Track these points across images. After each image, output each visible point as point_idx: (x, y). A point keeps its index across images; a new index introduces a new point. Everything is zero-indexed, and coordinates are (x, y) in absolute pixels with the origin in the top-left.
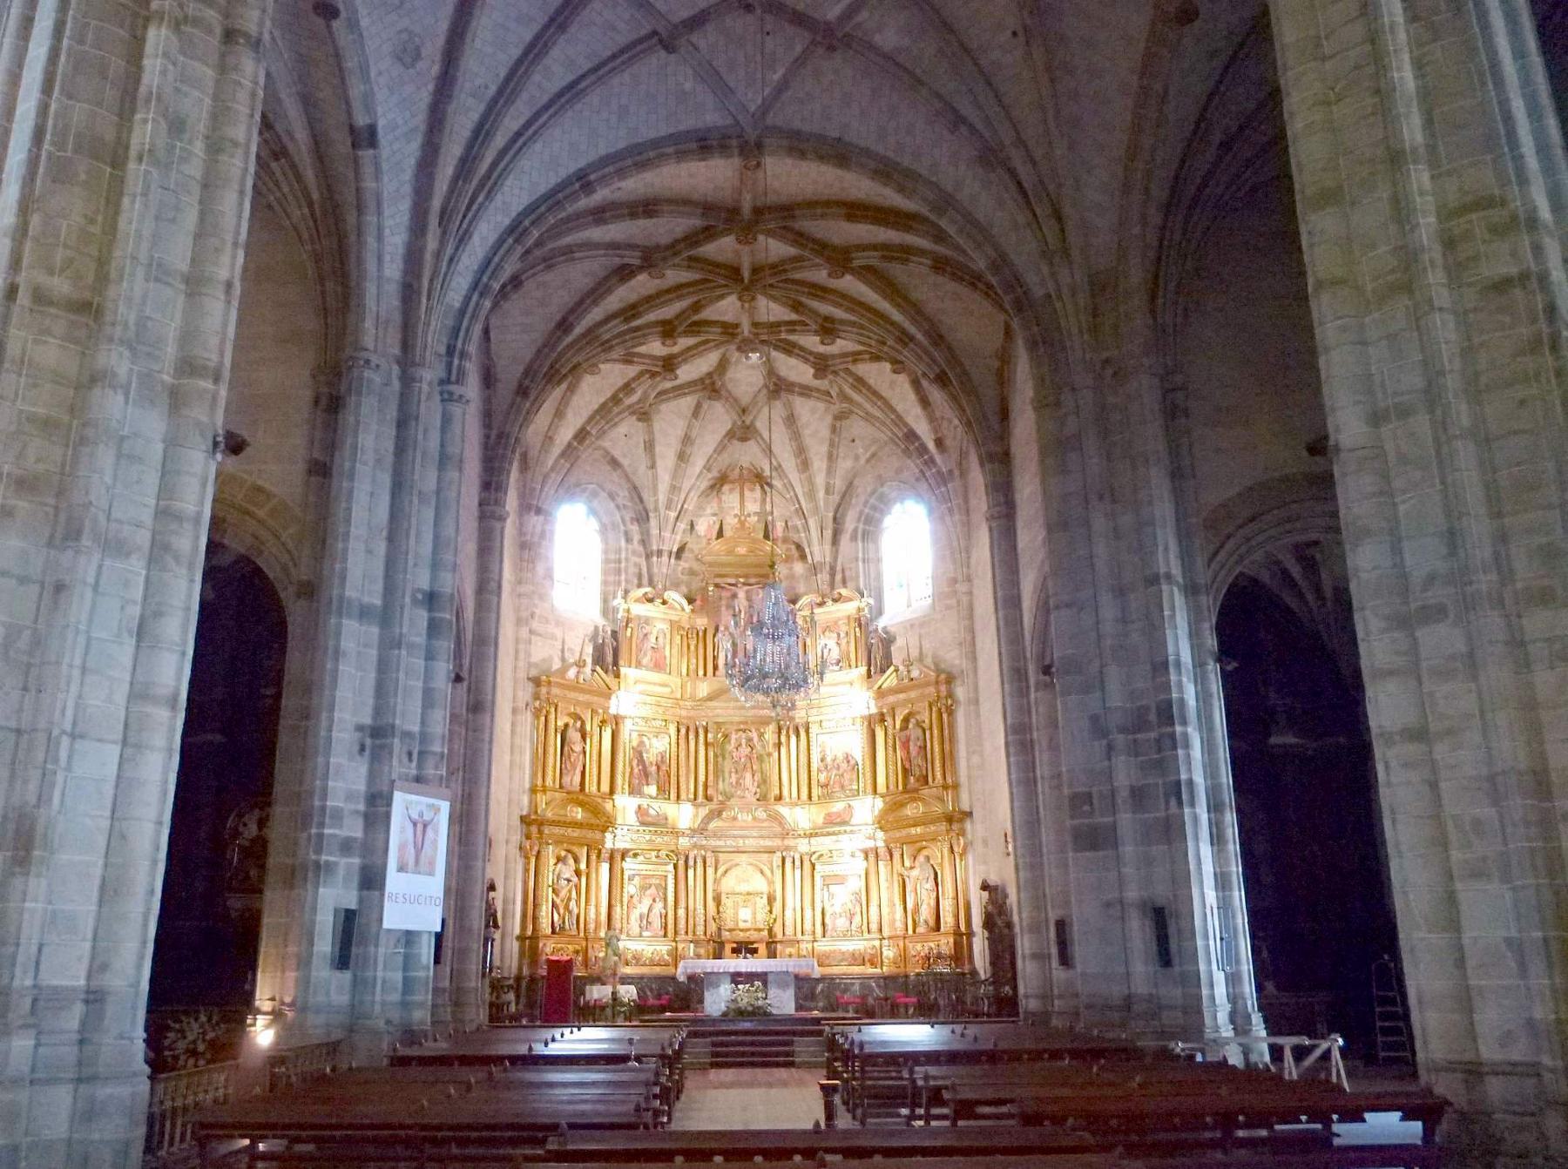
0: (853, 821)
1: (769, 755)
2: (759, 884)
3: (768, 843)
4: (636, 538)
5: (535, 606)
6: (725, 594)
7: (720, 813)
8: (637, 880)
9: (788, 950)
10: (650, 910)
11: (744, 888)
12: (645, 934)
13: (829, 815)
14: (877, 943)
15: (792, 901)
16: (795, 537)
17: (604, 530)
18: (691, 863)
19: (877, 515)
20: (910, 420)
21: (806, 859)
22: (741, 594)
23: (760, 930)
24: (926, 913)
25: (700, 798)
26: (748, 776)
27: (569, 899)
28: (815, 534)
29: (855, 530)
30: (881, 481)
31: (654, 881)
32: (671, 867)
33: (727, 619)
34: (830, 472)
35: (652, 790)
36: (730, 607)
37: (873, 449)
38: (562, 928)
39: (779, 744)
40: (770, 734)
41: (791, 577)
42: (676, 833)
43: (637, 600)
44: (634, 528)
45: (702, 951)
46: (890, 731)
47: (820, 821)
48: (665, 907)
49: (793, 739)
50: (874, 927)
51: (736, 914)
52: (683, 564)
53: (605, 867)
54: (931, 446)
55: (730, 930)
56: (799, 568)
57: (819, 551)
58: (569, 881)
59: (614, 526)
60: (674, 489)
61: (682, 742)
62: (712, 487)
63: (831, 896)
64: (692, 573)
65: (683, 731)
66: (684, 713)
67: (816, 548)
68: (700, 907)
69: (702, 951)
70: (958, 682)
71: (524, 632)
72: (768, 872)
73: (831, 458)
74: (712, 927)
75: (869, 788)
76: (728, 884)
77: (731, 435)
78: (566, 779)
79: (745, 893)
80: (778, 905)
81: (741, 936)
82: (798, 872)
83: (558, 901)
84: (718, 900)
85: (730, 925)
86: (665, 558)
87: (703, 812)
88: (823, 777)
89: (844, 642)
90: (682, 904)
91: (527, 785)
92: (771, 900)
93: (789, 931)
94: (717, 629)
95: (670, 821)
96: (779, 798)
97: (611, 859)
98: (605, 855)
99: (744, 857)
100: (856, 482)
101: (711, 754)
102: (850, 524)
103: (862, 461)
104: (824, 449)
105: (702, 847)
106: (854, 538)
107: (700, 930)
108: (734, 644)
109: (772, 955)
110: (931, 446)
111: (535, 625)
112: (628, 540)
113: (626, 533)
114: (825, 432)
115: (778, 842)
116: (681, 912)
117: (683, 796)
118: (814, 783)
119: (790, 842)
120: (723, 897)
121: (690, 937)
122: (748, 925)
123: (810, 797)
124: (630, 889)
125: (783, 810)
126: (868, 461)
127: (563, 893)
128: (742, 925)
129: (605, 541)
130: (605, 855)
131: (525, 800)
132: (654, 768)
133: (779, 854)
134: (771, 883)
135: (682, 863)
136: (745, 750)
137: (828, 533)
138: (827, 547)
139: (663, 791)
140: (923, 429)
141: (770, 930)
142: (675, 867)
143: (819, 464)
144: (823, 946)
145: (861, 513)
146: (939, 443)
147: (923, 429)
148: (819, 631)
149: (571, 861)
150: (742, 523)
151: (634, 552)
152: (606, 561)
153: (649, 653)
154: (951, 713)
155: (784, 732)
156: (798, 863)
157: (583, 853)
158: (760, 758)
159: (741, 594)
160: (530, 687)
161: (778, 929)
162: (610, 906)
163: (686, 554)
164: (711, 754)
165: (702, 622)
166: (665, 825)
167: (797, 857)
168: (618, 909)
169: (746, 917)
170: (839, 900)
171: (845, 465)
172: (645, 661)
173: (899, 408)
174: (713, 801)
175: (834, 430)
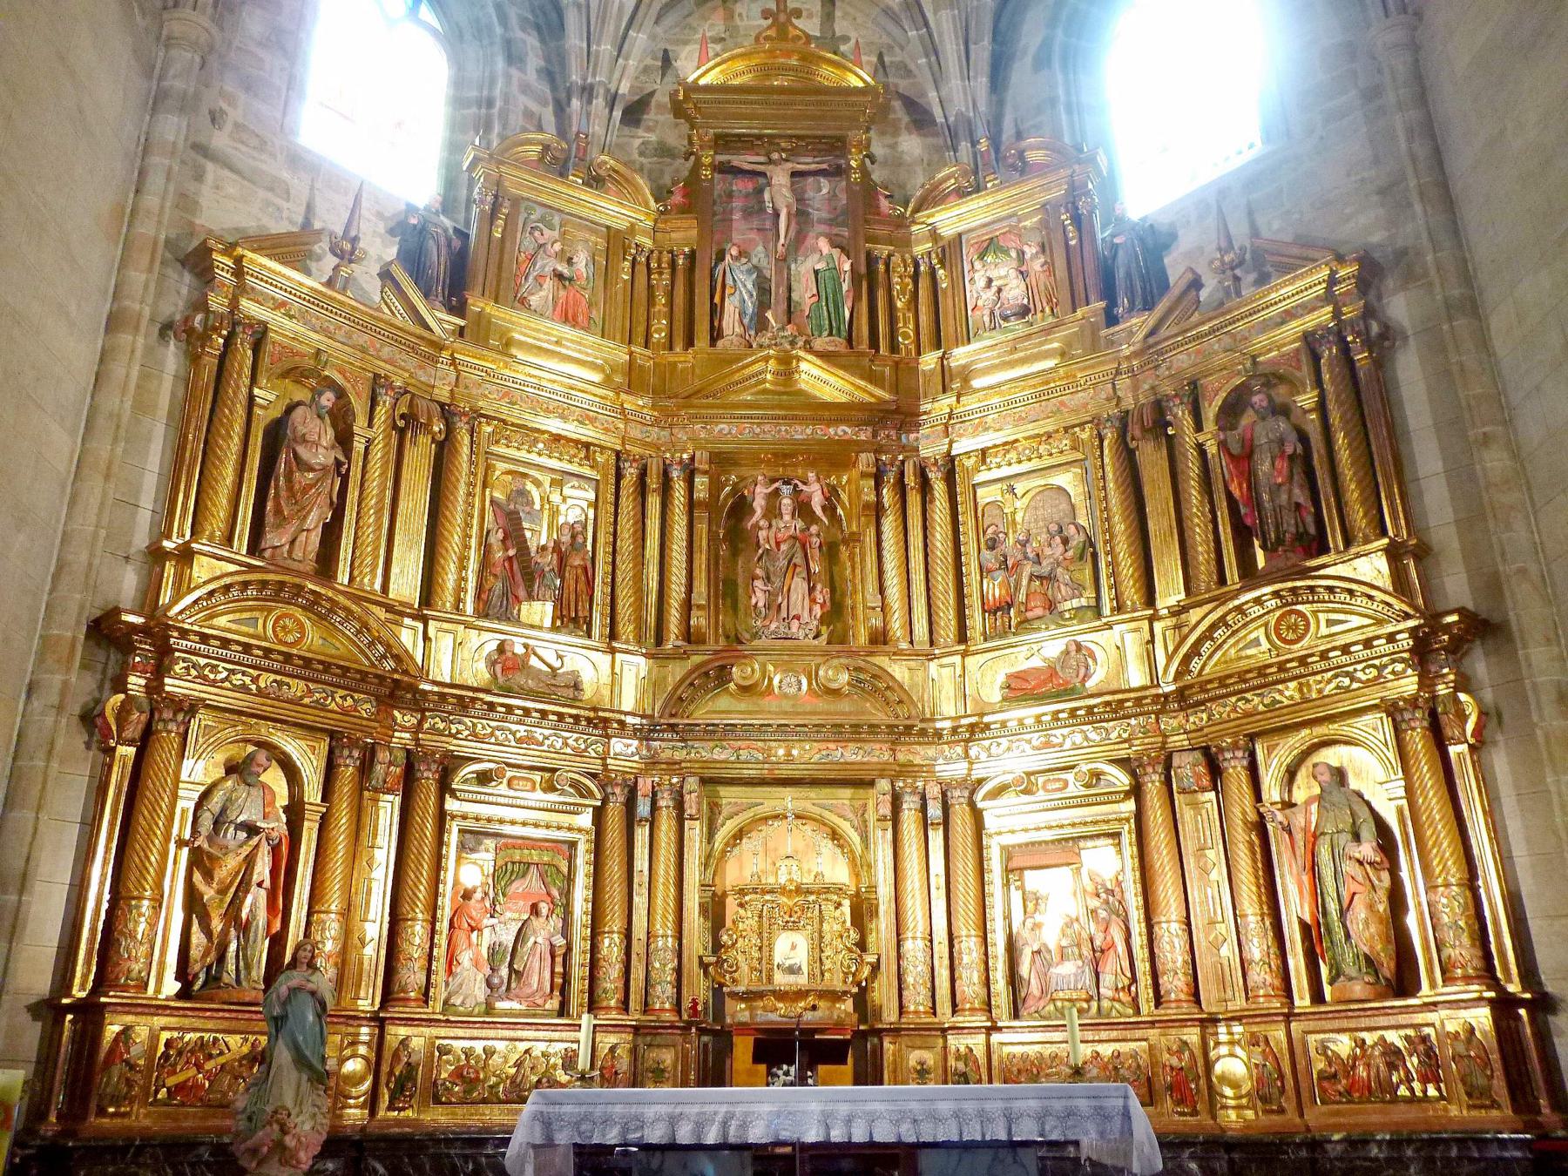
0: (1091, 684)
1: (855, 538)
2: (837, 871)
3: (850, 754)
4: (534, 62)
5: (232, 101)
6: (741, 186)
7: (723, 675)
8: (485, 857)
9: (914, 1057)
10: (520, 936)
11: (783, 876)
12: (501, 1005)
13: (1019, 676)
14: (1192, 1035)
15: (924, 912)
16: (903, 85)
17: (454, 38)
18: (643, 808)
21: (958, 797)
22: (780, 178)
23: (834, 996)
24: (1364, 930)
25: (673, 640)
26: (799, 586)
27: (244, 886)
28: (951, 49)
31: (535, 856)
32: (585, 820)
33: (741, 231)
35: (540, 611)
36: (755, 208)
38: (213, 980)
39: (878, 510)
40: (855, 485)
41: (896, 162)
42: (601, 722)
43: (524, 164)
44: (531, 43)
45: (667, 1057)
46: (1189, 438)
47: (994, 695)
48: (566, 930)
49: (914, 500)
50: (1175, 984)
51: (766, 948)
52: (643, 136)
53: (388, 809)
55: (750, 997)
56: (911, 145)
57: (958, 94)
58: (251, 830)
59: (480, 31)
61: (627, 504)
63: (1033, 901)
64: (663, 151)
65: (631, 472)
66: (635, 432)
67: (954, 84)
68: (664, 928)
69: (667, 1057)
70: (1390, 283)
71: (171, 127)
72: (855, 838)
74: (699, 989)
75: (1132, 594)
76: (742, 868)
78: (272, 538)
79: (791, 884)
80: (883, 926)
81: (776, 1014)
82: (936, 838)
83: (208, 893)
84: (715, 911)
85: (745, 980)
86: (599, 102)
87: (676, 671)
88: (995, 589)
89: (1037, 266)
90: (615, 923)
91: (141, 540)
92: (862, 912)
93: (917, 1000)
94: (721, 257)
95: (588, 693)
96: (880, 638)
97: (408, 785)
98: (387, 767)
99: (788, 799)
101: (702, 528)
105: (673, 766)
107: (663, 994)
108: (763, 289)
109: (870, 1073)
111: (220, 140)
112: (513, 57)
113: (508, 44)
115: (877, 753)
116: (611, 947)
117: (626, 629)
118: (973, 602)
119: (920, 754)
120: (731, 903)
121: (634, 1017)
122: (802, 981)
123: (962, 638)
124: (470, 871)
125: (899, 671)
127: (230, 865)
128: (781, 980)
129: (457, 62)
130: (387, 767)
131: (128, 583)
132: (548, 561)
133: (884, 785)
134: (860, 865)
135: (621, 809)
136: (789, 523)
137: (982, 51)
138: (983, 81)
139: (571, 618)
141: (861, 999)
142: (599, 815)
144: (1019, 1041)
148: (969, 253)
149: (275, 779)
150: (782, 31)
151: (525, 89)
152: (458, 102)
153: (549, 284)
154: (1381, 363)
155: (891, 477)
156: (935, 811)
157: (308, 758)
158: (831, 552)
159: (780, 178)
160: (184, 284)
161: (883, 993)
162: (396, 921)
163: (651, 116)
164: (702, 528)
165: (684, 234)
166: (573, 702)
167: (934, 791)
168: (417, 931)
169: (792, 958)
170: (1056, 908)
172: (534, 300)
174: (705, 653)
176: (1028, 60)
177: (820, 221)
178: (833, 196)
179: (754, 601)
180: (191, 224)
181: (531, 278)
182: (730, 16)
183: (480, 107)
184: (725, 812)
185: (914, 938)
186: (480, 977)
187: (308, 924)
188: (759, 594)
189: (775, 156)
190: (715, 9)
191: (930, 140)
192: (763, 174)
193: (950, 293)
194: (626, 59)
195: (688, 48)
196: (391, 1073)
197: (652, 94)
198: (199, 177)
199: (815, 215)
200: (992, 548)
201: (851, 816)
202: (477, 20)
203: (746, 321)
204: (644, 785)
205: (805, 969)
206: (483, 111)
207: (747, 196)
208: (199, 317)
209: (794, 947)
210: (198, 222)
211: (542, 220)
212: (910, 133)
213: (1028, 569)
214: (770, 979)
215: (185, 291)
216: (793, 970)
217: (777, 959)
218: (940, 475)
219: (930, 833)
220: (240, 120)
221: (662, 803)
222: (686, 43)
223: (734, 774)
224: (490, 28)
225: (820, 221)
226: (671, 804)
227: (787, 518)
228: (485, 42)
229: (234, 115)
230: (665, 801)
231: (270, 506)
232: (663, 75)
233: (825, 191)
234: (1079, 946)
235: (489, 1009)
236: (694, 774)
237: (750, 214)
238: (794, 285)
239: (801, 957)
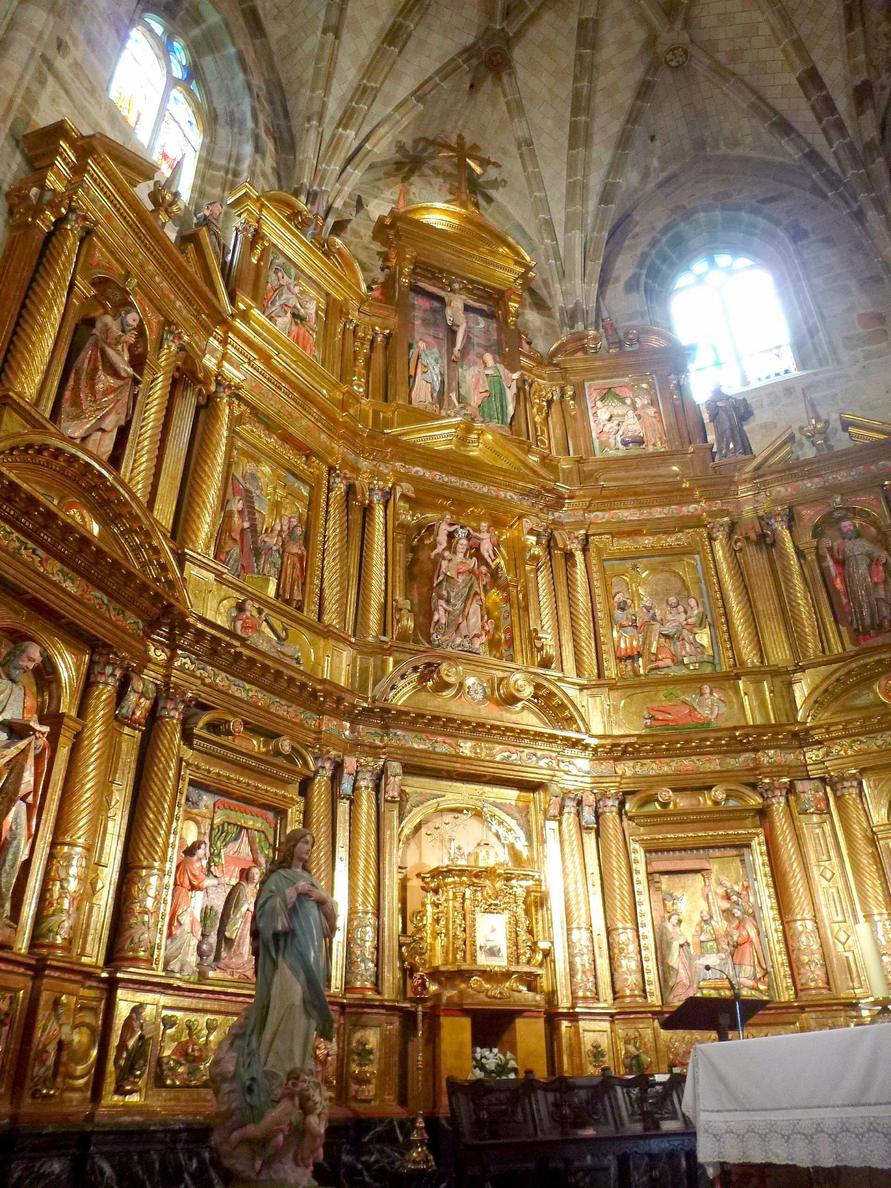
12: (211, 974)
18: (346, 786)
19: (664, 267)
20: (817, 55)
29: (635, 278)
30: (687, 214)
34: (616, 167)
37: (672, 168)
54: (843, 103)
60: (362, 92)
62: (399, 165)
73: (624, 141)
77: (469, 52)
100: (636, 217)
102: (624, 267)
103: (651, 185)
104: (615, 127)
106: (632, 286)
110: (843, 103)
111: (62, 64)
114: (625, 98)
122: (500, 963)
126: (660, 185)
128: (483, 961)
137: (595, 268)
140: (836, 74)
143: (601, 152)
145: (645, 255)
146: (862, 94)
147: (836, 74)
156: (588, 816)
171: (631, 177)
173: (804, 32)
175: (644, 90)
176: (621, 286)
177: (479, 345)
178: (487, 331)
179: (436, 618)
180: (28, 116)
181: (278, 304)
182: (405, 193)
183: (227, 172)
184: (412, 800)
185: (579, 928)
186: (194, 942)
187: (51, 857)
188: (442, 612)
189: (456, 286)
190: (396, 183)
191: (546, 319)
192: (441, 300)
193: (579, 417)
194: (343, 185)
195: (376, 201)
196: (122, 1046)
197: (349, 221)
198: (42, 82)
199: (476, 340)
200: (623, 609)
201: (517, 815)
202: (232, 113)
203: (435, 395)
204: (350, 763)
205: (504, 952)
206: (230, 177)
207: (425, 311)
208: (34, 190)
209: (493, 930)
210: (34, 117)
211: (283, 266)
212: (532, 309)
213: (657, 627)
214: (474, 960)
215: (14, 167)
216: (493, 952)
217: (479, 942)
218: (579, 547)
219: (584, 835)
220: (80, 61)
221: (363, 783)
222: (375, 197)
223: (429, 764)
224: (242, 123)
225: (479, 345)
226: (371, 785)
227: (461, 555)
228: (236, 130)
229: (76, 53)
230: (366, 782)
231: (67, 394)
232: (357, 212)
233: (481, 326)
234: (716, 940)
235: (202, 976)
236: (396, 760)
237: (428, 324)
238: (462, 384)
239: (501, 940)
